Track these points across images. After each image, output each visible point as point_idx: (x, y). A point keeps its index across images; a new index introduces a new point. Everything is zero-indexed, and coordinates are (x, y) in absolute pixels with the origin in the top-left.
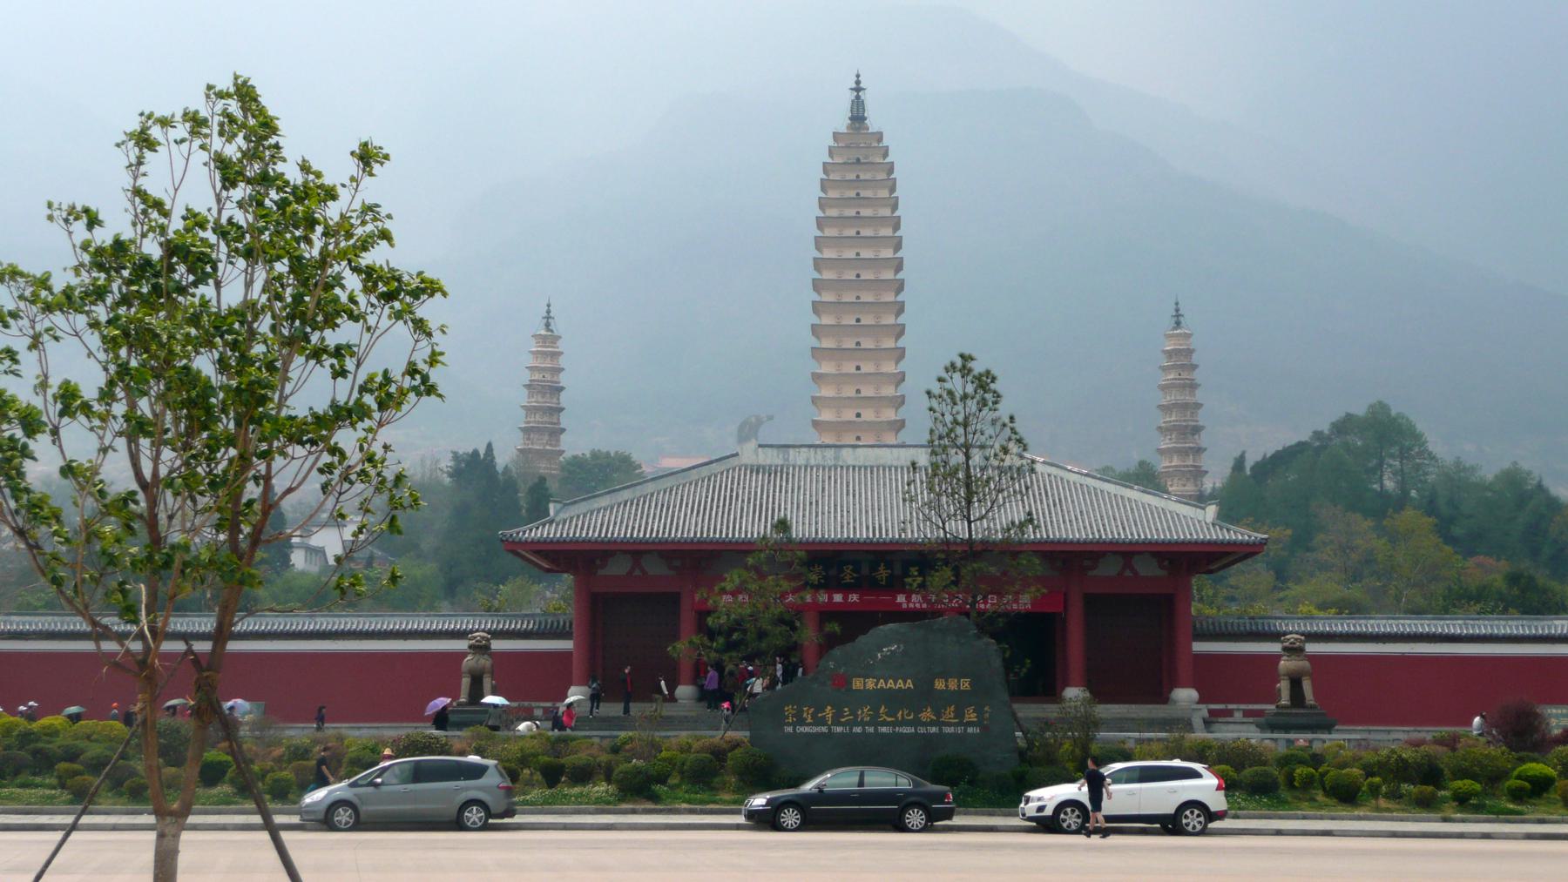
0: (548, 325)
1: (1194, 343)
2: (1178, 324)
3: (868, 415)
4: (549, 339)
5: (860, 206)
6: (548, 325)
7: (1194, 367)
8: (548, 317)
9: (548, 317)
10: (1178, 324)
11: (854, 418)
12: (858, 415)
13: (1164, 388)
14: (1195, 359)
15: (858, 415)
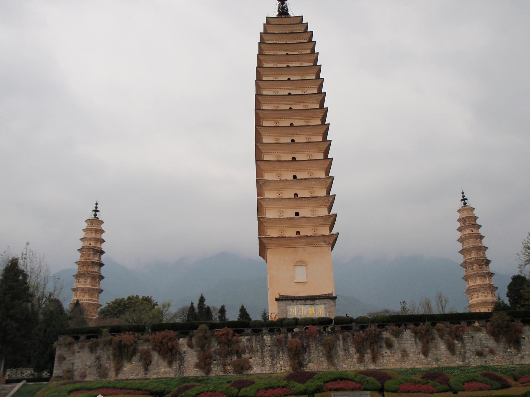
0: (95, 215)
1: (476, 213)
2: (465, 204)
3: (305, 213)
4: (95, 225)
5: (288, 61)
6: (95, 215)
7: (479, 226)
8: (96, 211)
9: (96, 211)
10: (465, 204)
11: (294, 216)
12: (297, 214)
13: (461, 240)
14: (478, 222)
15: (297, 214)
